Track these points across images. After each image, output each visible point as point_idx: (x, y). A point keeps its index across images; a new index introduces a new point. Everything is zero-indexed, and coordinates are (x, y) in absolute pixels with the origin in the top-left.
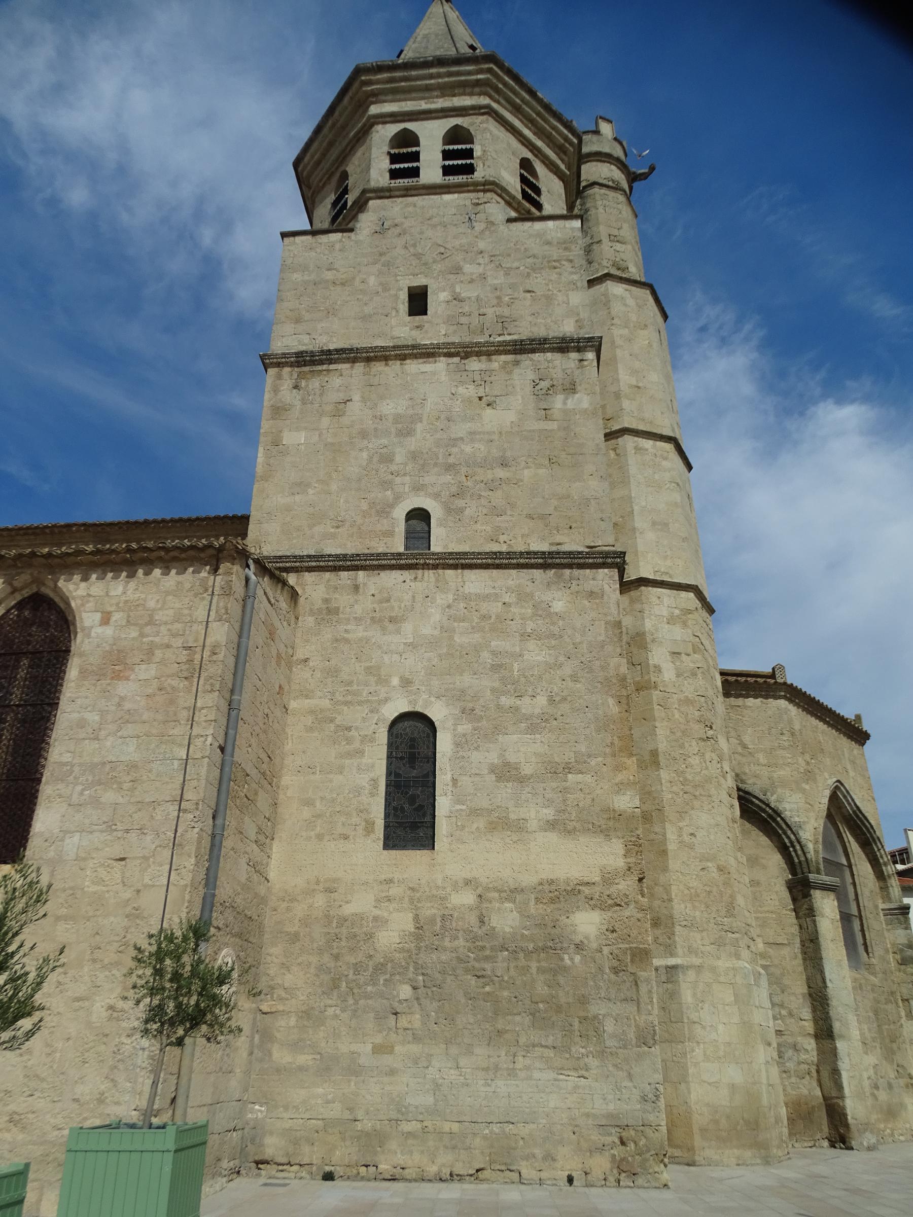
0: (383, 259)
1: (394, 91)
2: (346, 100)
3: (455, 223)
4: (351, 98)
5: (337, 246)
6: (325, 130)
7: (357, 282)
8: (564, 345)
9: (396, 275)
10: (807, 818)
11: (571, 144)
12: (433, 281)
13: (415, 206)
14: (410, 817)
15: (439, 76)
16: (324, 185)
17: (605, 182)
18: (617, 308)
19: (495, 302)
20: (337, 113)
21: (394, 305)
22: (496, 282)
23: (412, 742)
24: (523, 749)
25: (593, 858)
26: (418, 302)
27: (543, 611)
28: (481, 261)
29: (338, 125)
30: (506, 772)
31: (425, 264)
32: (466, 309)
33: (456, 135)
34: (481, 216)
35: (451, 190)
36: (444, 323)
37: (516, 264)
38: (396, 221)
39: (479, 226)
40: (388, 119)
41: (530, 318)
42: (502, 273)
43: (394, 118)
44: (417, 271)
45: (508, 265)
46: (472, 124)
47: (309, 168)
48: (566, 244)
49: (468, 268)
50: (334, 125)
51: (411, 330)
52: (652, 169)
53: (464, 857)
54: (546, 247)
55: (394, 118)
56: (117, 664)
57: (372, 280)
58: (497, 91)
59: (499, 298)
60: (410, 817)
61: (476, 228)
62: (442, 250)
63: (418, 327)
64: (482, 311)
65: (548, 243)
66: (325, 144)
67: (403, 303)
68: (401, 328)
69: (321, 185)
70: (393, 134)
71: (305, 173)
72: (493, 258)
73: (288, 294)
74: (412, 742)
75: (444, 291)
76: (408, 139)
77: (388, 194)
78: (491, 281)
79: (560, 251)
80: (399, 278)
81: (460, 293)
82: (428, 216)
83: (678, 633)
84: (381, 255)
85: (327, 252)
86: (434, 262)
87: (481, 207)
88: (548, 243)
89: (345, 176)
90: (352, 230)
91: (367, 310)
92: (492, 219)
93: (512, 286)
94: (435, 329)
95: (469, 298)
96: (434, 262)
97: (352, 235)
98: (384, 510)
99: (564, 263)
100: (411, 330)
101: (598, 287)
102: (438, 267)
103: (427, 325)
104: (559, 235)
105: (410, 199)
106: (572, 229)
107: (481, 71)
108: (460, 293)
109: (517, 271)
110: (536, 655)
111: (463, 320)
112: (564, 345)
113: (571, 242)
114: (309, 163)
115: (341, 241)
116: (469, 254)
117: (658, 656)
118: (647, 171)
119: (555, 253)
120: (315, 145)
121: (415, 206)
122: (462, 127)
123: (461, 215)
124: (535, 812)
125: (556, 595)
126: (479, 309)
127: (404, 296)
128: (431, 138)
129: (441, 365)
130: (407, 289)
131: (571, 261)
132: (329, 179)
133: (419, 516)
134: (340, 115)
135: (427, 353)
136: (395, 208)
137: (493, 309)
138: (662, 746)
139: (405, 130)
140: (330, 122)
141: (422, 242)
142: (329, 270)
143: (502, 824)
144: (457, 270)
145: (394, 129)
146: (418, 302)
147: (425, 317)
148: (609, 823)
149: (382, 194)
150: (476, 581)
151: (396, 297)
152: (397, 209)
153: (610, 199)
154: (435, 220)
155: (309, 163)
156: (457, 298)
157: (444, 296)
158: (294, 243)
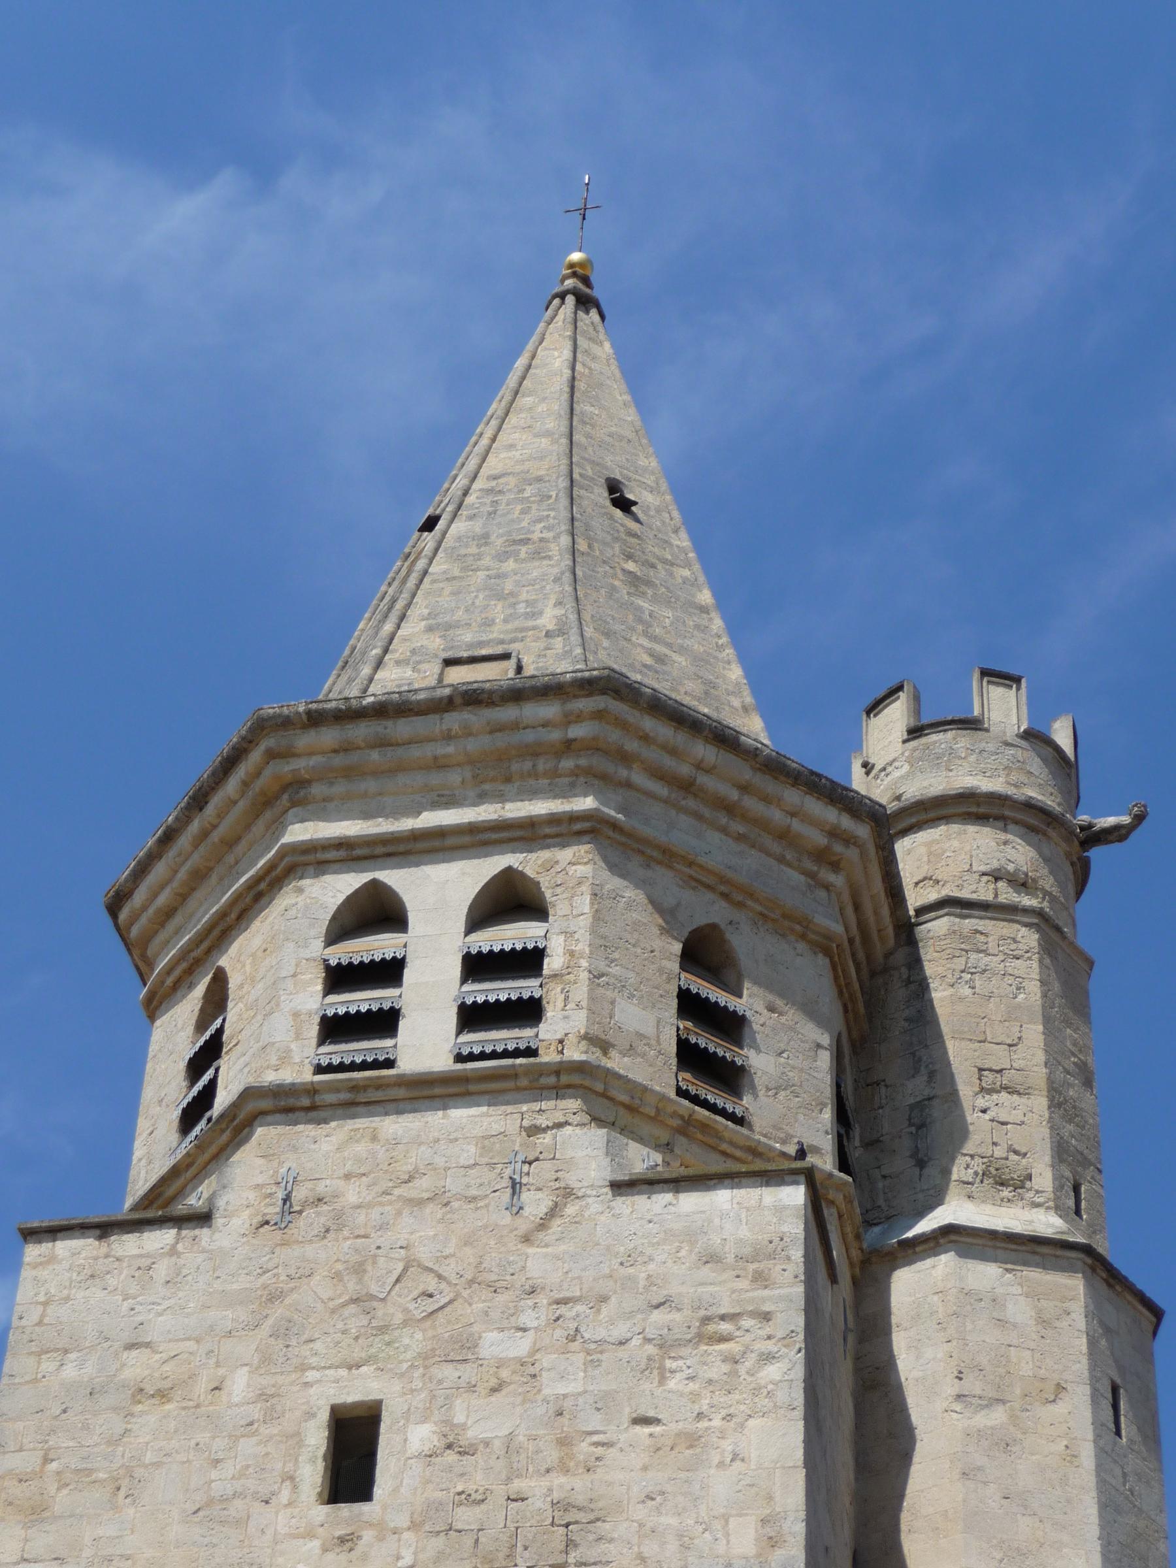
0: (278, 1312)
1: (350, 773)
2: (232, 785)
3: (474, 1192)
4: (246, 784)
5: (162, 1270)
6: (184, 841)
7: (202, 1386)
9: (303, 1368)
11: (849, 840)
12: (397, 1386)
13: (374, 1138)
15: (468, 733)
16: (176, 986)
17: (985, 893)
19: (552, 1455)
20: (210, 810)
21: (290, 1466)
22: (561, 1389)
28: (528, 1318)
29: (215, 836)
31: (383, 1329)
32: (477, 1482)
33: (509, 900)
34: (542, 1172)
35: (472, 1088)
36: (414, 1526)
37: (621, 1330)
38: (321, 1188)
39: (535, 1203)
40: (331, 855)
41: (640, 1512)
42: (579, 1358)
43: (349, 853)
44: (358, 1354)
45: (601, 1333)
46: (548, 867)
47: (143, 920)
48: (756, 1261)
49: (497, 1345)
50: (204, 834)
51: (325, 1550)
52: (1139, 819)
54: (706, 1272)
55: (349, 853)
57: (240, 1384)
58: (625, 758)
59: (564, 1442)
61: (526, 1212)
62: (431, 1284)
63: (342, 1540)
64: (518, 1485)
65: (711, 1259)
66: (182, 874)
67: (313, 1461)
69: (169, 981)
70: (341, 898)
71: (135, 932)
72: (563, 1310)
73: (20, 1425)
75: (425, 1420)
76: (379, 912)
77: (306, 1102)
78: (552, 1387)
79: (744, 1284)
80: (311, 1375)
81: (464, 1427)
82: (406, 1167)
84: (274, 1297)
85: (133, 1289)
86: (405, 1323)
87: (546, 1139)
88: (711, 1259)
89: (220, 980)
90: (204, 1218)
91: (222, 1480)
92: (570, 1179)
93: (603, 1403)
95: (487, 1443)
96: (405, 1323)
97: (204, 1233)
99: (747, 1323)
100: (325, 1550)
101: (929, 1262)
102: (413, 1341)
103: (368, 1535)
104: (744, 1232)
105: (361, 1123)
106: (779, 1210)
107: (570, 719)
108: (464, 1427)
109: (623, 1353)
111: (466, 1517)
113: (771, 1256)
114: (144, 908)
115: (173, 1252)
116: (502, 1298)
118: (1126, 819)
119: (725, 1292)
120: (160, 870)
121: (374, 1138)
122: (522, 874)
123: (492, 1166)
126: (509, 1480)
127: (317, 1438)
128: (439, 900)
130: (324, 1416)
131: (766, 1317)
132: (190, 971)
134: (221, 816)
136: (323, 1151)
137: (545, 1482)
139: (374, 883)
140: (195, 826)
141: (381, 1260)
142: (131, 1346)
144: (463, 1349)
145: (337, 888)
147: (364, 1507)
149: (291, 1102)
151: (296, 1438)
152: (326, 1146)
153: (992, 947)
154: (422, 1186)
155: (144, 908)
156: (454, 1445)
157: (422, 1436)
158: (52, 1259)
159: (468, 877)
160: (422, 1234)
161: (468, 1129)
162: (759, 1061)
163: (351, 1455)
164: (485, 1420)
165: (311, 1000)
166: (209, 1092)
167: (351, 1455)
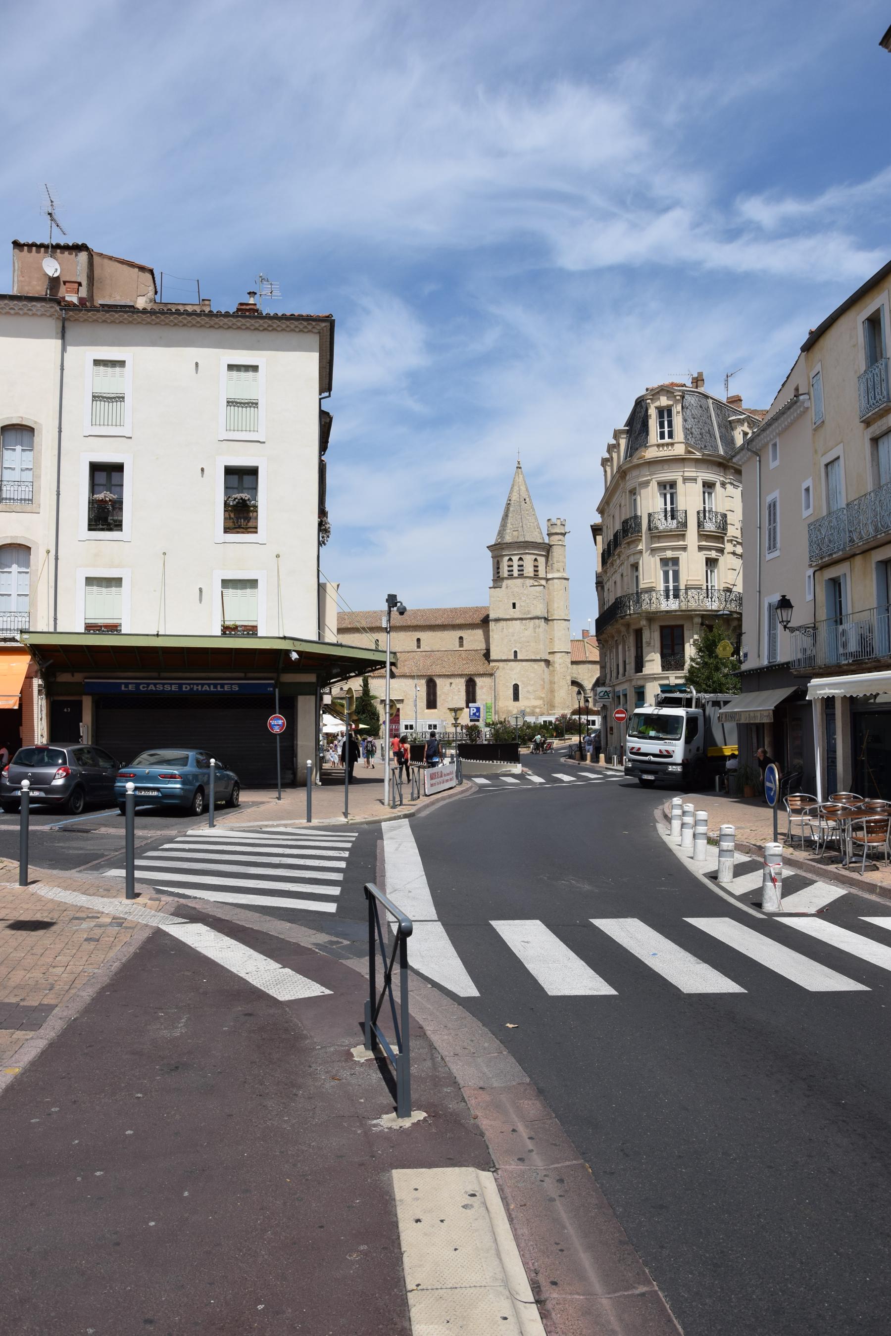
8: (538, 618)
10: (588, 684)
14: (516, 698)
18: (556, 586)
23: (516, 688)
24: (531, 689)
25: (538, 703)
26: (514, 605)
27: (533, 668)
30: (528, 692)
33: (521, 559)
48: (540, 592)
49: (523, 599)
53: (523, 703)
56: (482, 687)
60: (516, 698)
68: (512, 613)
74: (516, 688)
76: (510, 560)
83: (561, 660)
94: (516, 613)
98: (510, 651)
110: (533, 675)
112: (538, 618)
117: (557, 665)
119: (538, 595)
124: (532, 697)
125: (535, 665)
128: (515, 559)
129: (518, 622)
133: (516, 652)
135: (516, 619)
136: (509, 582)
138: (556, 680)
143: (528, 699)
145: (508, 558)
146: (514, 605)
148: (541, 698)
150: (524, 663)
159: (518, 557)
160: (516, 590)
161: (519, 581)
162: (539, 568)
163: (514, 605)
164: (523, 604)
165: (506, 568)
166: (498, 573)
167: (514, 605)
